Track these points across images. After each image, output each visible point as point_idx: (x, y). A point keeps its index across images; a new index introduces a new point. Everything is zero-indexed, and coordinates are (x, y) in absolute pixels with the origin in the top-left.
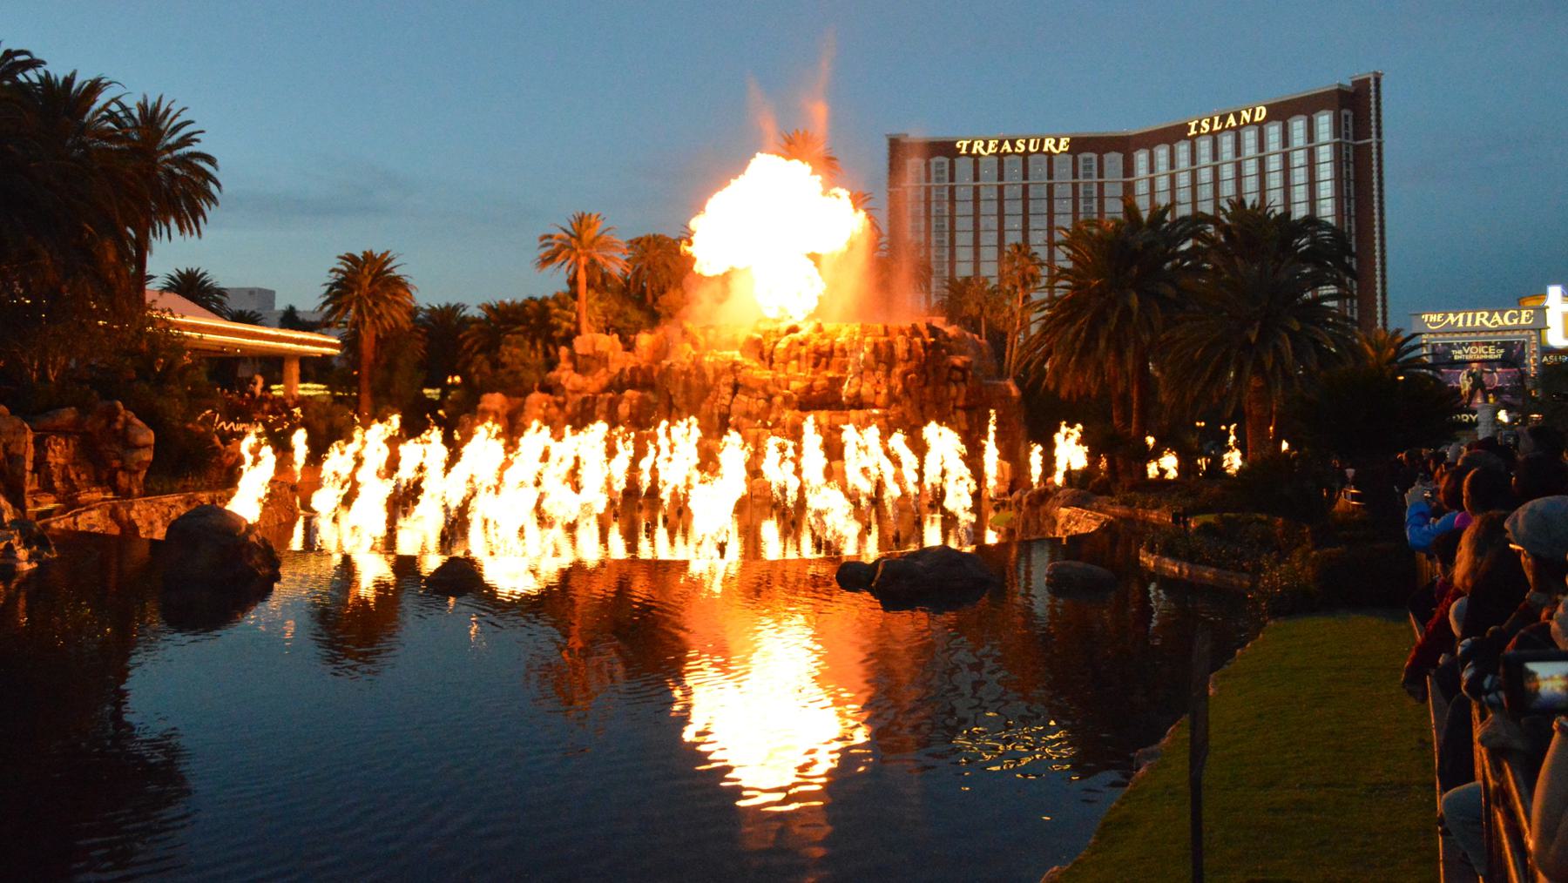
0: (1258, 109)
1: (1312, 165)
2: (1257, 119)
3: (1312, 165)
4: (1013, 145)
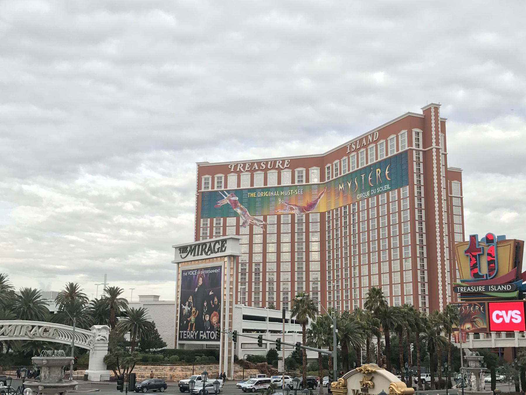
0: (375, 133)
2: (375, 139)
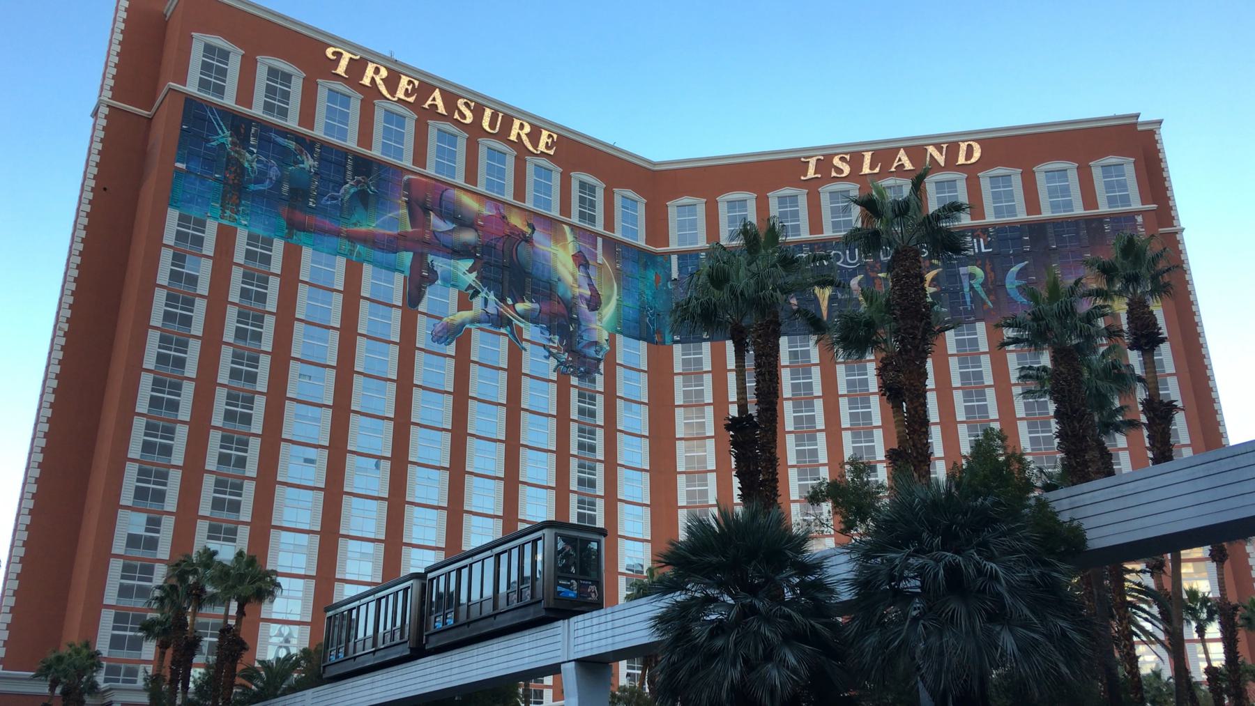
1: (167, 384)
3: (167, 384)
4: (450, 99)
